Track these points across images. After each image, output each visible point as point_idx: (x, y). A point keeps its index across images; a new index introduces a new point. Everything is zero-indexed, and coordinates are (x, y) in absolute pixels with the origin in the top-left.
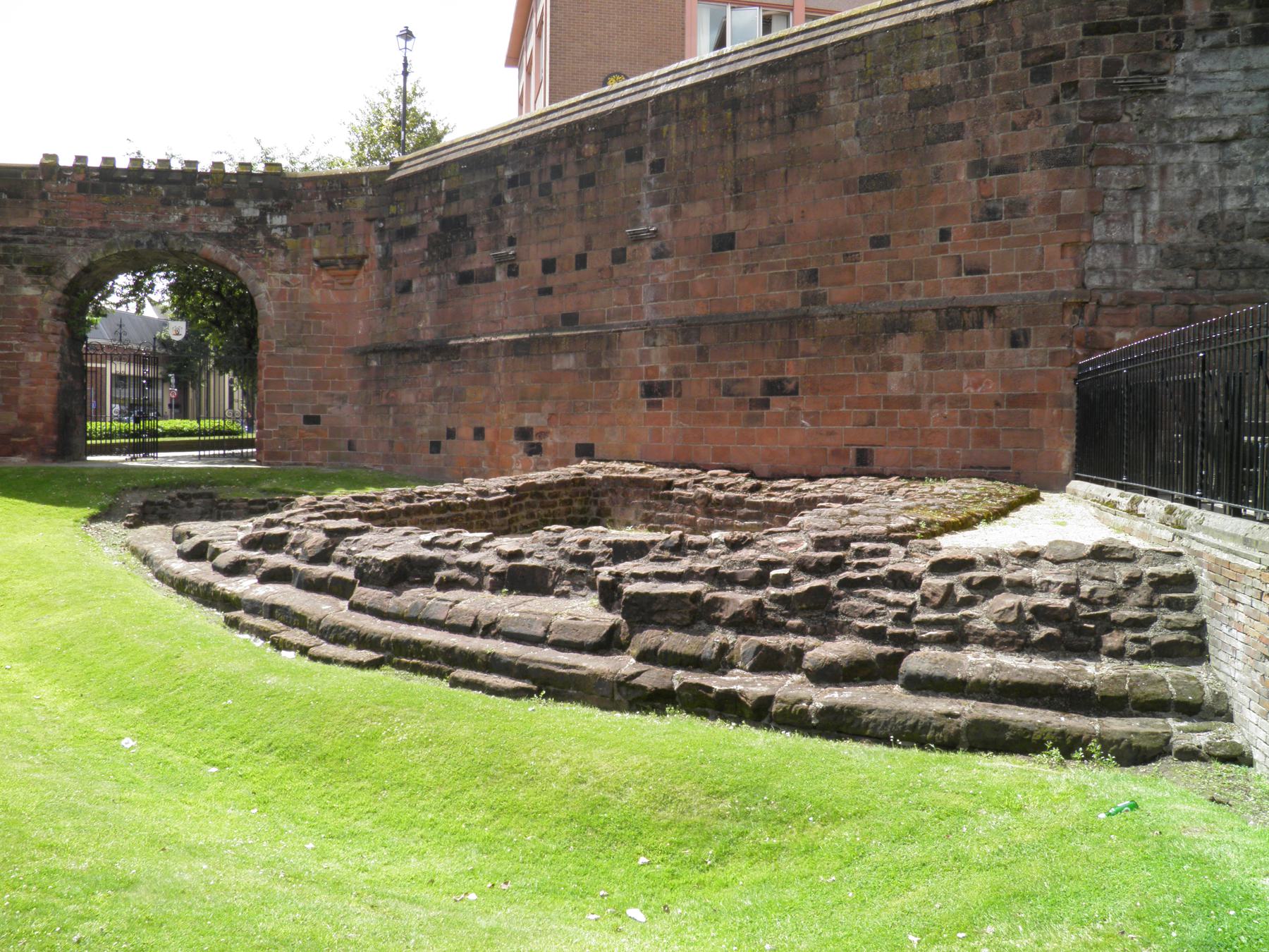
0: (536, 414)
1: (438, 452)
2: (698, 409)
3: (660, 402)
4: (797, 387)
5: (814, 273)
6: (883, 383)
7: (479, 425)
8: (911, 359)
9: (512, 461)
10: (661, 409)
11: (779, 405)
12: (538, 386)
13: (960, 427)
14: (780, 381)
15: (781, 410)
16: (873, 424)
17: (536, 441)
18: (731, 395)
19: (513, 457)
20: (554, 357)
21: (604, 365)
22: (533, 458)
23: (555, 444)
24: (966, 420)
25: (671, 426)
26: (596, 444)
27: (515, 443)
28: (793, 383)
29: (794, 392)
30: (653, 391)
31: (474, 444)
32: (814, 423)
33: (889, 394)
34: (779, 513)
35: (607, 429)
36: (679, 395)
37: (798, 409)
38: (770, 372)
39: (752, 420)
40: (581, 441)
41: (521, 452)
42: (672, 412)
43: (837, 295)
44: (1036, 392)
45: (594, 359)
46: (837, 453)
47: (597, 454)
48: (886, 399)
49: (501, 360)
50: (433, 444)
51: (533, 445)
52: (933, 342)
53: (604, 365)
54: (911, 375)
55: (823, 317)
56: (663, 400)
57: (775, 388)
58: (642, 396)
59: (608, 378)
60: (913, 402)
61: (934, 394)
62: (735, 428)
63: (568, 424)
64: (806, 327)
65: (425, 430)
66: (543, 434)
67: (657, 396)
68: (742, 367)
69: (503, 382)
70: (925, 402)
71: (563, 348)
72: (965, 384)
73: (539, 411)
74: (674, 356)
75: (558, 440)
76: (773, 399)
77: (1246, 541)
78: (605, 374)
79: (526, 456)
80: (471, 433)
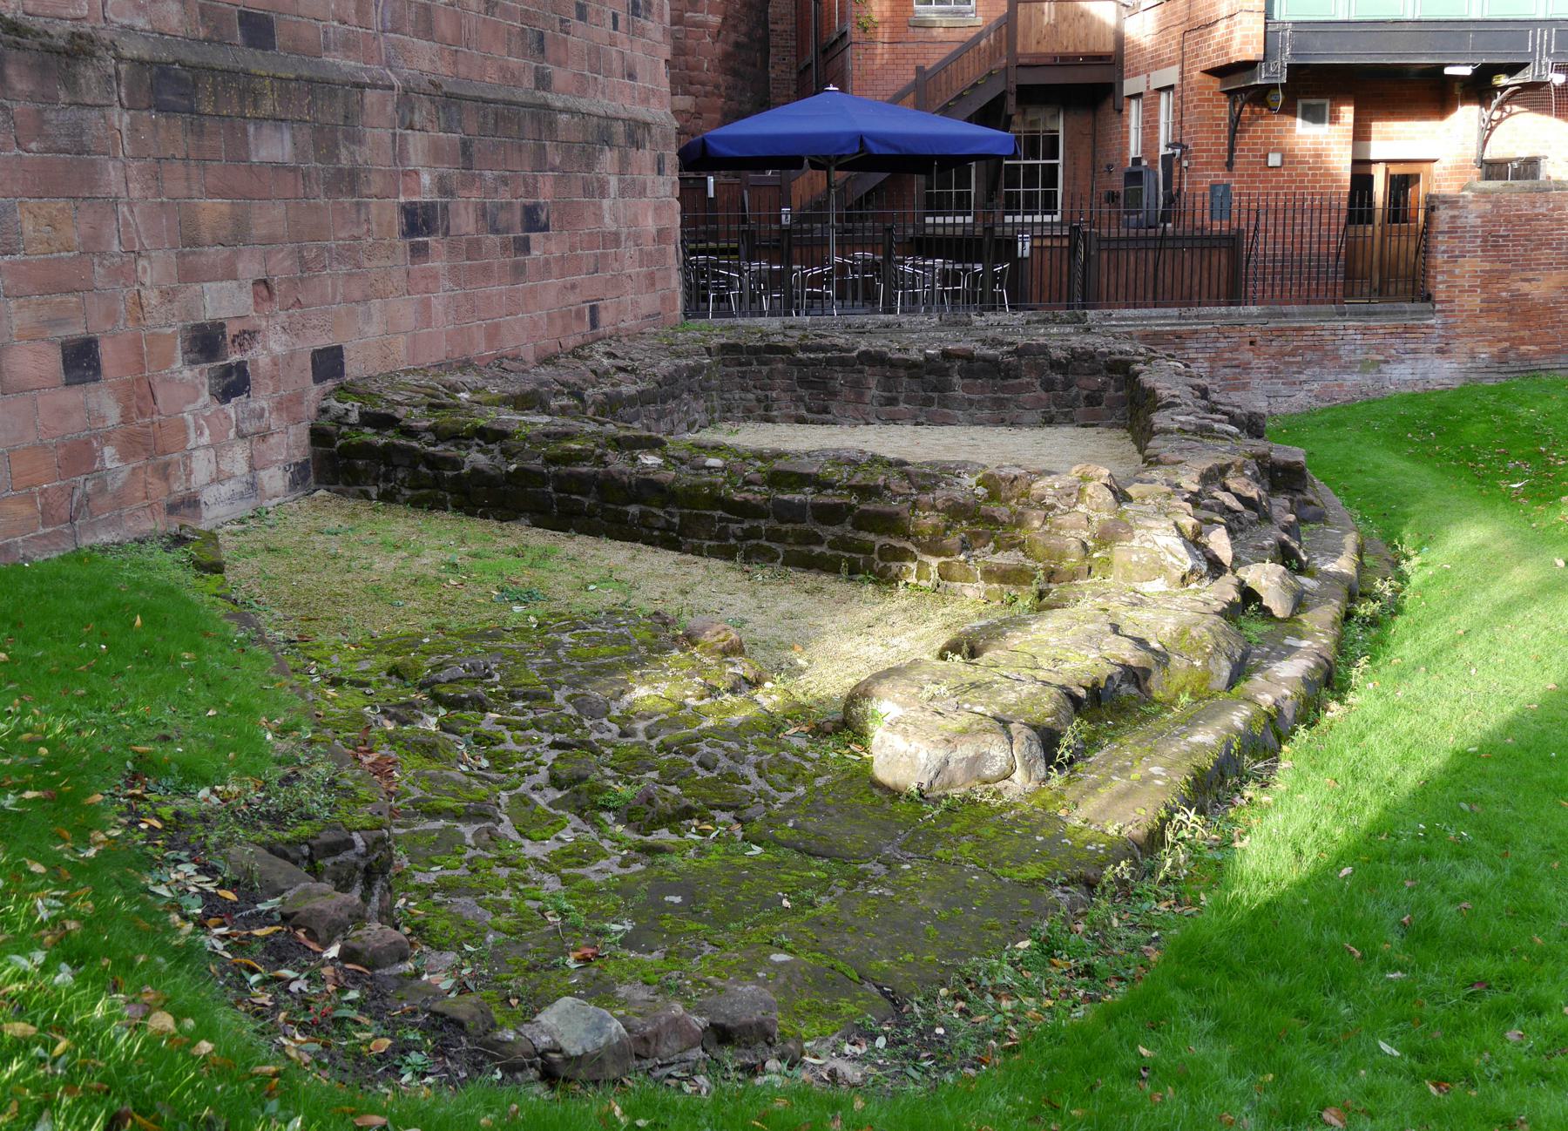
2: (468, 259)
3: (426, 244)
5: (541, 37)
6: (599, 217)
7: (77, 331)
8: (613, 182)
12: (223, 205)
17: (234, 358)
20: (251, 129)
21: (345, 162)
26: (345, 345)
27: (187, 374)
29: (546, 228)
30: (419, 221)
31: (71, 397)
35: (360, 309)
36: (446, 233)
38: (528, 194)
39: (518, 271)
41: (205, 396)
43: (560, 76)
45: (325, 141)
46: (579, 315)
49: (121, 119)
51: (228, 370)
52: (623, 165)
53: (345, 162)
55: (561, 111)
57: (533, 220)
59: (353, 191)
60: (615, 239)
64: (551, 123)
66: (248, 337)
68: (505, 181)
69: (136, 190)
71: (268, 106)
73: (231, 275)
74: (436, 153)
76: (533, 235)
77: (1180, 317)
78: (348, 181)
79: (216, 406)
80: (53, 362)
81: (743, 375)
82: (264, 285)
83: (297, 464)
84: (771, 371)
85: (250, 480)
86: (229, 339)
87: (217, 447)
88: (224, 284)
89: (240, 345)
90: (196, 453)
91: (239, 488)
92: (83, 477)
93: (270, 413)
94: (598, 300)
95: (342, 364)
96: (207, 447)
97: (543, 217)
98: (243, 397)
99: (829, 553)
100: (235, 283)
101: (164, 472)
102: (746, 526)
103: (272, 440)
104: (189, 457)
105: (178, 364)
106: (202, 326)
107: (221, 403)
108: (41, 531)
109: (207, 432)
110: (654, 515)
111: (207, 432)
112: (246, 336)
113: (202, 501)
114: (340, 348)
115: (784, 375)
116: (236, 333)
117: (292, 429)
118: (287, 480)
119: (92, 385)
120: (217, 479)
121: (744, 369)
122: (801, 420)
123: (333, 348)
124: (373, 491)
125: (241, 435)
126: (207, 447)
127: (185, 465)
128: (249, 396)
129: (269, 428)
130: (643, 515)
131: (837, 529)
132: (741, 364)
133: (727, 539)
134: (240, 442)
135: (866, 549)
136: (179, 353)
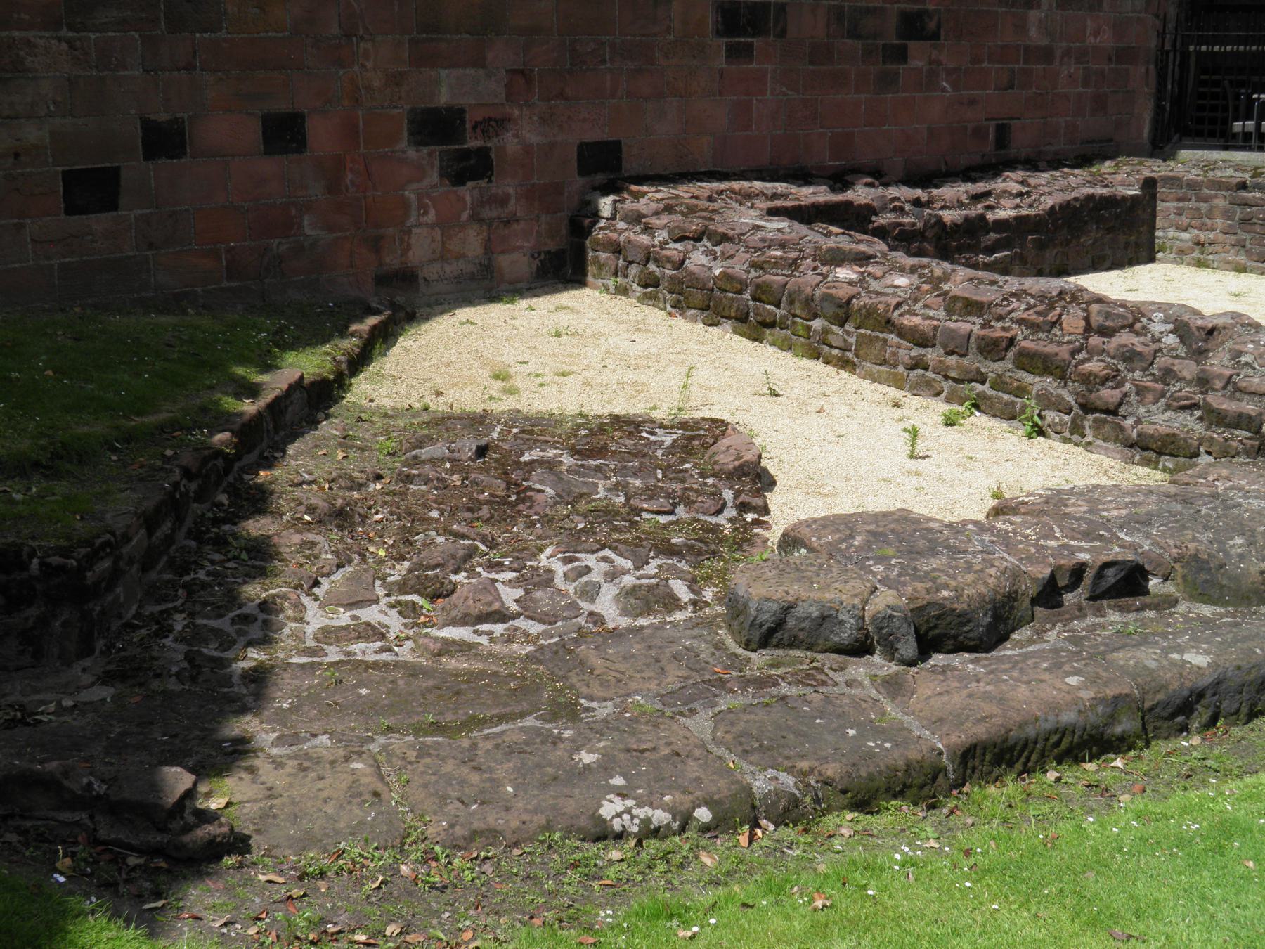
0: (471, 71)
1: (110, 203)
2: (812, 63)
3: (751, 44)
4: (939, 27)
7: (281, 106)
9: (405, 205)
10: (751, 62)
11: (919, 56)
13: (1081, 89)
14: (921, 15)
15: (920, 64)
16: (1012, 87)
17: (473, 143)
18: (858, 37)
19: (409, 194)
22: (468, 192)
23: (528, 149)
24: (1086, 83)
25: (769, 96)
27: (412, 153)
28: (936, 19)
29: (935, 36)
32: (955, 87)
33: (1028, 43)
34: (1030, 232)
36: (782, 34)
37: (939, 63)
40: (592, 136)
41: (434, 177)
42: (769, 67)
44: (1134, 45)
46: (979, 133)
47: (630, 165)
48: (1027, 48)
50: (71, 178)
51: (466, 154)
54: (1046, 16)
56: (755, 41)
58: (718, 34)
60: (1046, 55)
61: (1064, 44)
62: (863, 96)
63: (561, 95)
65: (32, 134)
66: (495, 124)
67: (745, 34)
70: (1058, 53)
72: (1088, 32)
73: (478, 62)
75: (533, 138)
76: (913, 45)
80: (252, 132)
81: (1179, 212)
82: (520, 76)
83: (549, 252)
84: (1211, 209)
85: (486, 263)
86: (468, 126)
87: (446, 225)
88: (468, 71)
89: (483, 131)
90: (415, 230)
91: (470, 268)
92: (277, 241)
93: (517, 199)
94: (1012, 118)
95: (619, 160)
96: (432, 226)
97: (932, 25)
98: (483, 183)
99: (990, 392)
100: (481, 72)
101: (376, 245)
102: (913, 353)
103: (515, 226)
104: (409, 232)
105: (403, 144)
106: (435, 112)
107: (454, 185)
108: (225, 284)
109: (432, 212)
110: (833, 333)
111: (432, 212)
112: (492, 123)
113: (421, 275)
114: (617, 144)
115: (1227, 214)
116: (479, 119)
117: (543, 218)
118: (534, 267)
119: (295, 156)
120: (443, 257)
121: (1181, 204)
122: (1241, 269)
123: (607, 143)
124: (611, 283)
125: (476, 218)
126: (432, 226)
127: (402, 240)
128: (490, 181)
129: (515, 214)
130: (825, 331)
131: (998, 366)
132: (1179, 200)
133: (895, 366)
134: (476, 226)
135: (1021, 391)
136: (405, 134)
